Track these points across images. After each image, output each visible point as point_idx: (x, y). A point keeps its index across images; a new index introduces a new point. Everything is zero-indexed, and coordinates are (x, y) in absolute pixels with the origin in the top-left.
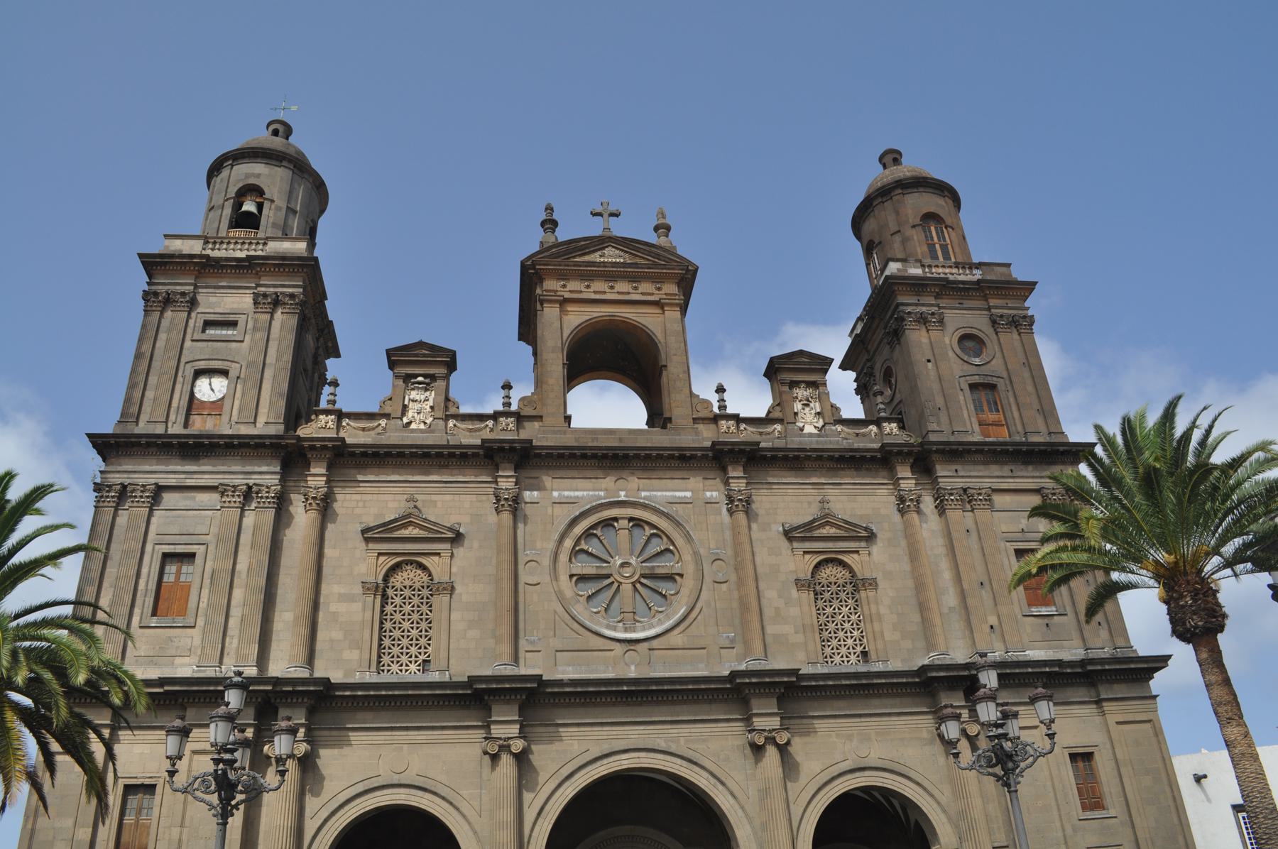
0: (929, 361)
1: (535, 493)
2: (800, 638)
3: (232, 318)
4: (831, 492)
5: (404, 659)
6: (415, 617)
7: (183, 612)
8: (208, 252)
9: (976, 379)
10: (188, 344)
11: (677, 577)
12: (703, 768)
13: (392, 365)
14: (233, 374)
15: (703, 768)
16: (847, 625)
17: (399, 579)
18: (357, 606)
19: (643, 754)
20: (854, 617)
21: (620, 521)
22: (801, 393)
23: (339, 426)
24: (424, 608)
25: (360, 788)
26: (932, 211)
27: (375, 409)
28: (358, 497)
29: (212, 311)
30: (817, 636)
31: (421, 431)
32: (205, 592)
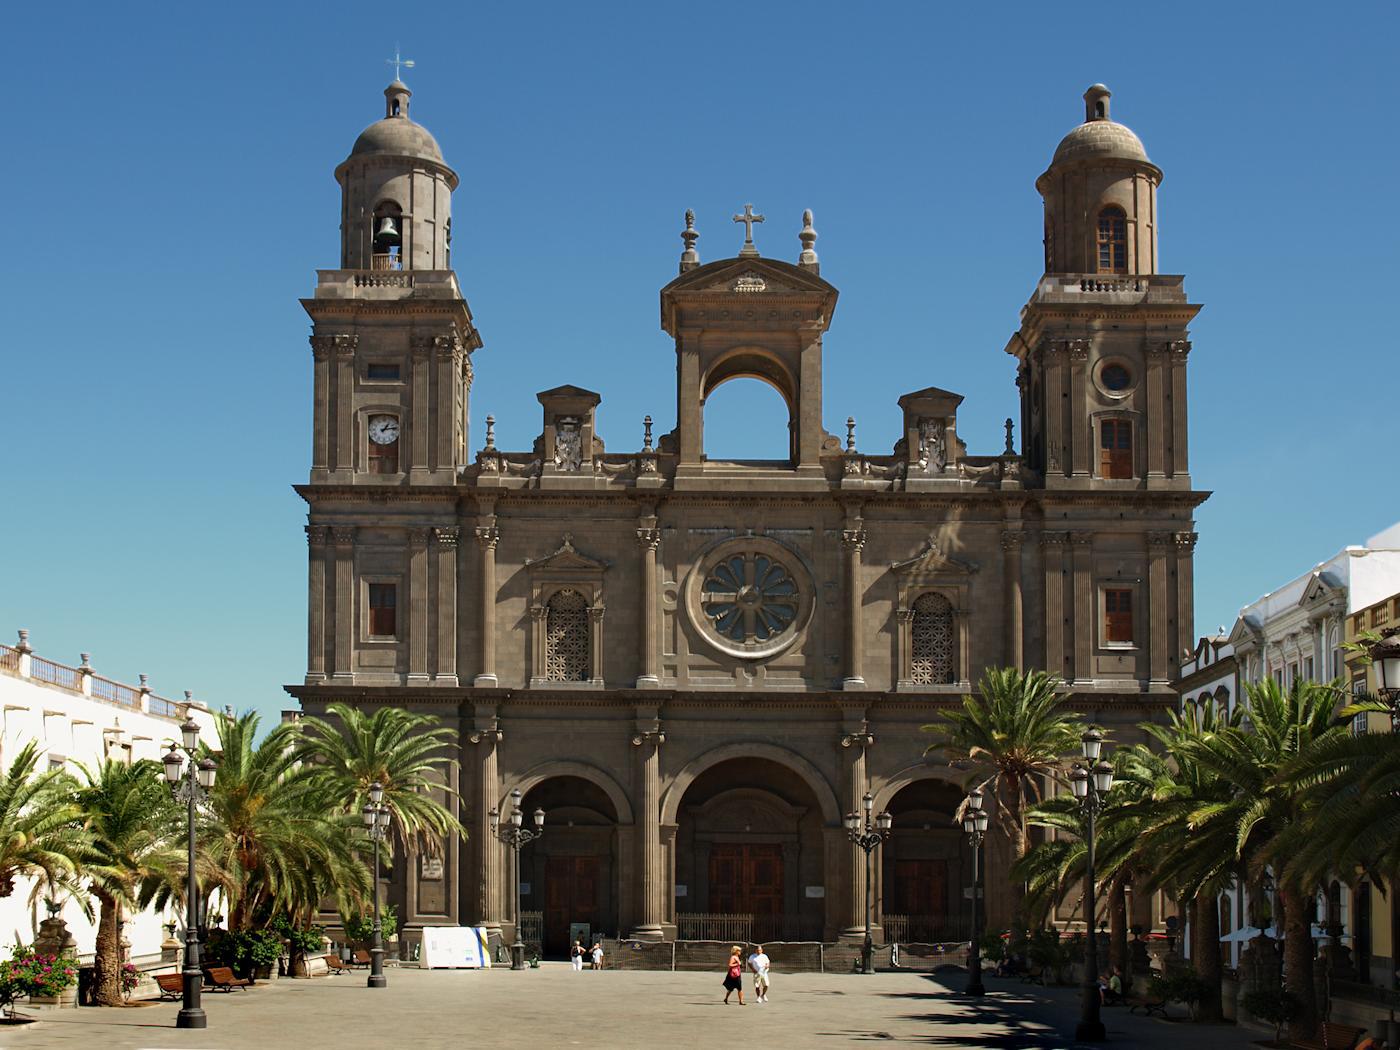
3: (394, 361)
6: (574, 635)
19: (754, 746)
23: (501, 468)
24: (582, 629)
26: (1114, 201)
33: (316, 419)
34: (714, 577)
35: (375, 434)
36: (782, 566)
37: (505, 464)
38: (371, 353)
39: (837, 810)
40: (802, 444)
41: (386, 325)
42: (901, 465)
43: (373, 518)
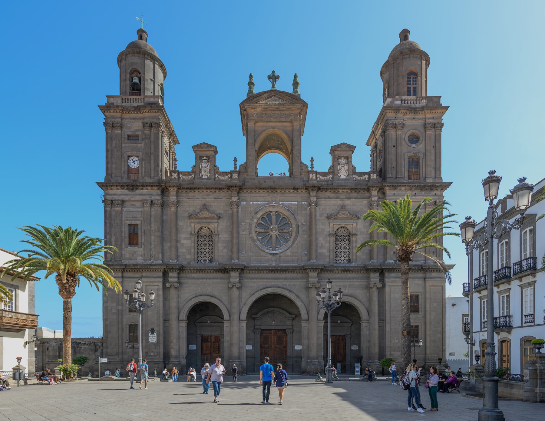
0: (394, 146)
1: (245, 203)
2: (327, 254)
3: (137, 133)
4: (347, 202)
5: (205, 258)
6: (208, 245)
7: (137, 244)
8: (124, 104)
9: (412, 154)
10: (123, 145)
11: (290, 232)
12: (294, 293)
13: (195, 152)
14: (141, 157)
15: (294, 293)
16: (345, 250)
17: (202, 233)
18: (189, 242)
19: (275, 289)
20: (348, 247)
21: (273, 213)
22: (342, 161)
24: (210, 242)
25: (194, 296)
27: (190, 170)
28: (186, 204)
29: (129, 130)
30: (334, 253)
31: (206, 179)
32: (143, 237)
33: (107, 157)
34: (261, 222)
35: (131, 164)
36: (286, 217)
37: (180, 176)
38: (128, 130)
39: (307, 314)
40: (294, 167)
41: (134, 119)
42: (331, 176)
43: (129, 197)
